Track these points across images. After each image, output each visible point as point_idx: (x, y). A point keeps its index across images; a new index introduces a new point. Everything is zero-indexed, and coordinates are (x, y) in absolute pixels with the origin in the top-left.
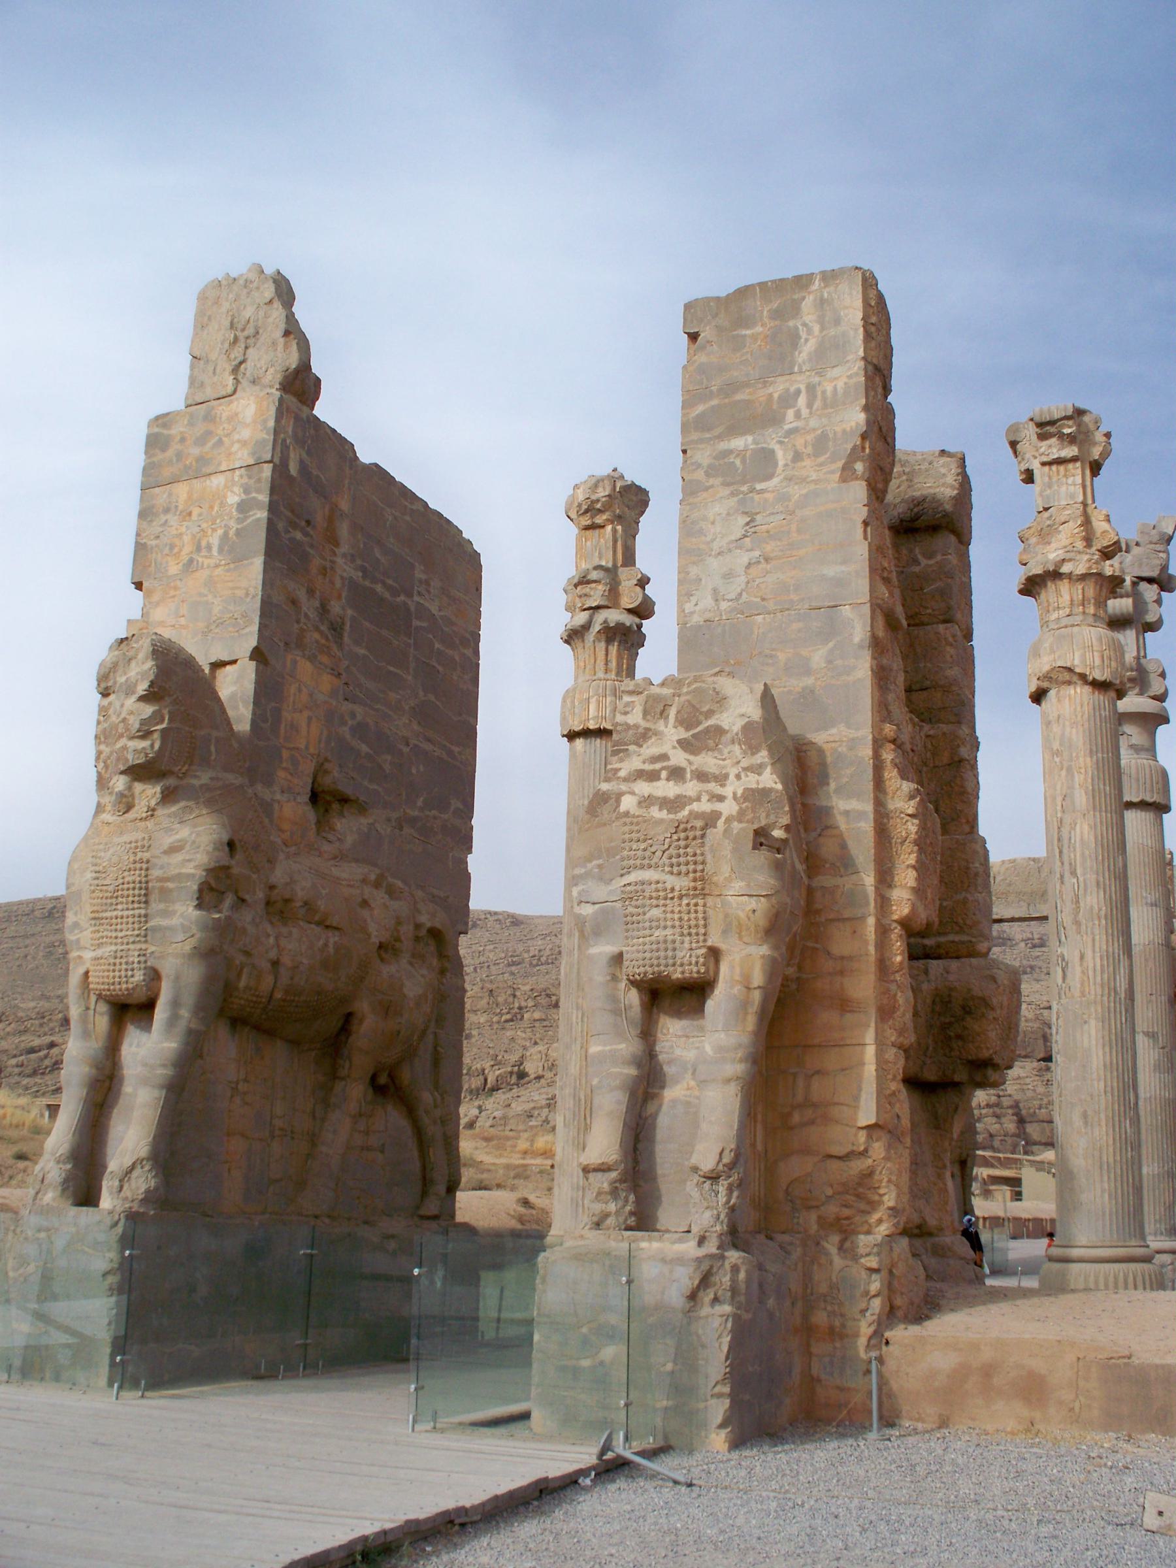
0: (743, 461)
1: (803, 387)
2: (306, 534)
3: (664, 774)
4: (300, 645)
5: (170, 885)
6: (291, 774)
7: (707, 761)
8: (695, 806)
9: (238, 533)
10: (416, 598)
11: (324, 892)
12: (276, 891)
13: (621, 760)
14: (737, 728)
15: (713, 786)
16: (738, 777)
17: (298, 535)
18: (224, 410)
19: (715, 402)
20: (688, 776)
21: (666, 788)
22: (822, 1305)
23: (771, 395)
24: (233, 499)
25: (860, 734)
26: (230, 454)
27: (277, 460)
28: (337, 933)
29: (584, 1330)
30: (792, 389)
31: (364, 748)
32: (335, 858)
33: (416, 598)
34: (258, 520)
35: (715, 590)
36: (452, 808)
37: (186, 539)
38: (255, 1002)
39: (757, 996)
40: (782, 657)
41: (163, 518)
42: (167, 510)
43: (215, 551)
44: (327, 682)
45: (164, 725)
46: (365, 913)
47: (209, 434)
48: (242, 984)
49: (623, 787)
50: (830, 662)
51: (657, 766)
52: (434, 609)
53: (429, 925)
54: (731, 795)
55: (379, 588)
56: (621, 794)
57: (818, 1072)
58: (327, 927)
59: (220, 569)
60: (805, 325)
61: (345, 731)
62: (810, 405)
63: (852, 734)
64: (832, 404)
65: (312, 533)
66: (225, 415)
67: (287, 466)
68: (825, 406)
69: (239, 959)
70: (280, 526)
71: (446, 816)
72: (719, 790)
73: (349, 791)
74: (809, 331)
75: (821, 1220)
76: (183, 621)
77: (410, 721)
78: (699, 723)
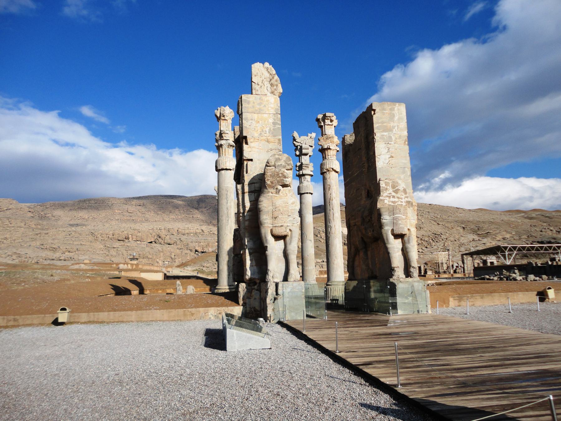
1: (396, 125)
3: (391, 197)
8: (398, 203)
15: (400, 200)
19: (380, 124)
21: (392, 199)
23: (390, 126)
24: (271, 121)
29: (406, 295)
35: (383, 162)
37: (258, 128)
41: (251, 121)
42: (252, 120)
43: (267, 133)
51: (390, 195)
62: (398, 129)
66: (265, 100)
72: (401, 201)
74: (397, 114)
76: (260, 148)
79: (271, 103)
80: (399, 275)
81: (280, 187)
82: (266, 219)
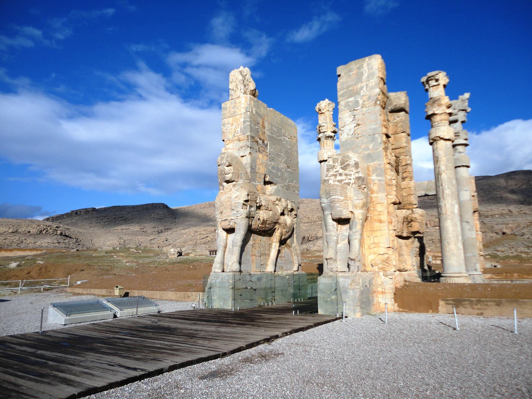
0: (352, 103)
1: (365, 85)
2: (258, 126)
3: (338, 175)
5: (236, 205)
7: (347, 172)
9: (244, 128)
13: (329, 173)
14: (353, 164)
15: (349, 177)
16: (354, 174)
17: (257, 127)
18: (238, 101)
19: (345, 90)
20: (343, 175)
21: (339, 178)
22: (380, 286)
23: (357, 87)
24: (242, 120)
25: (381, 162)
26: (240, 110)
27: (250, 111)
29: (328, 293)
30: (362, 86)
31: (274, 171)
32: (270, 195)
33: (283, 137)
34: (248, 124)
35: (347, 134)
36: (294, 182)
37: (232, 130)
39: (361, 221)
40: (363, 147)
41: (227, 125)
42: (228, 124)
43: (239, 132)
44: (265, 158)
45: (232, 171)
46: (277, 206)
47: (235, 106)
49: (330, 178)
50: (373, 147)
51: (337, 173)
54: (352, 178)
55: (275, 136)
56: (329, 180)
57: (375, 236)
59: (240, 136)
60: (365, 70)
61: (270, 168)
62: (366, 89)
63: (379, 163)
64: (372, 88)
68: (370, 89)
70: (252, 125)
71: (293, 184)
73: (271, 181)
74: (366, 71)
75: (379, 268)
76: (234, 148)
78: (345, 163)
79: (242, 103)
80: (332, 268)
81: (225, 184)
82: (217, 214)
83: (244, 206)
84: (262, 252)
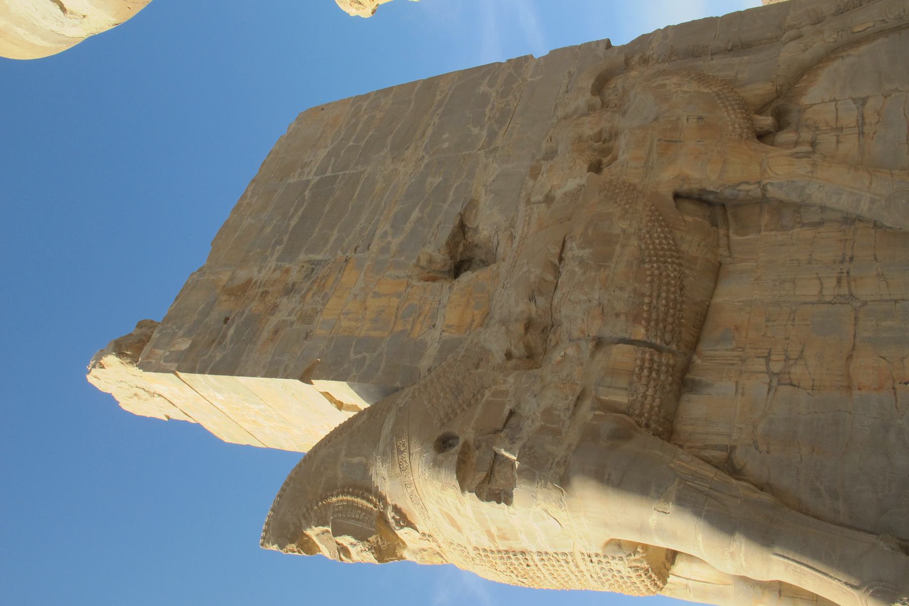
4: (307, 318)
6: (419, 316)
10: (311, 178)
11: (525, 269)
12: (515, 352)
17: (231, 331)
28: (568, 245)
31: (415, 214)
38: (650, 369)
48: (621, 398)
52: (322, 153)
53: (588, 95)
55: (293, 223)
58: (561, 259)
65: (233, 315)
67: (183, 352)
69: (586, 412)
77: (403, 160)
83: (499, 483)
84: (828, 294)
